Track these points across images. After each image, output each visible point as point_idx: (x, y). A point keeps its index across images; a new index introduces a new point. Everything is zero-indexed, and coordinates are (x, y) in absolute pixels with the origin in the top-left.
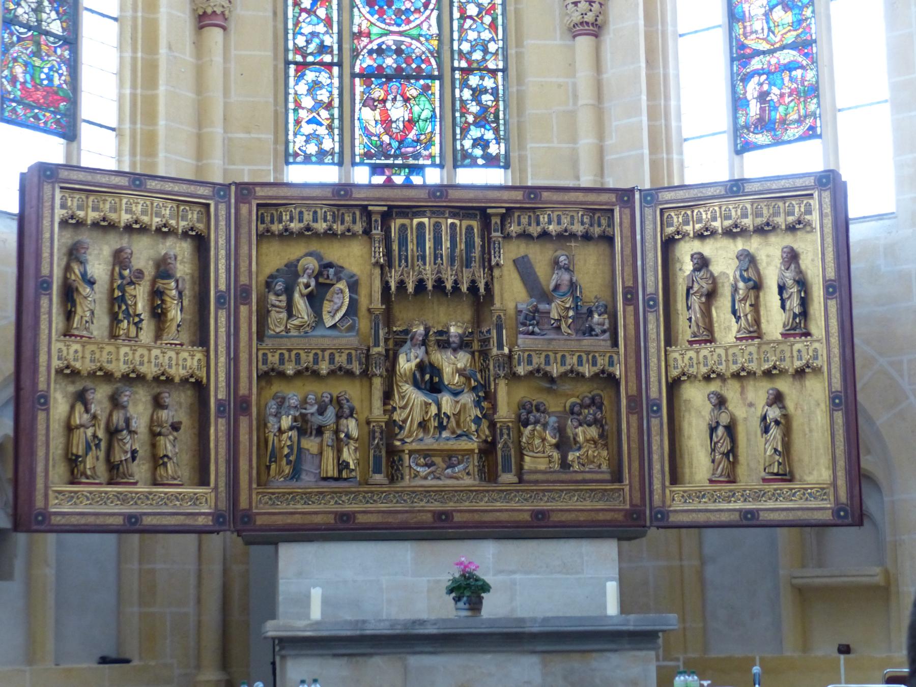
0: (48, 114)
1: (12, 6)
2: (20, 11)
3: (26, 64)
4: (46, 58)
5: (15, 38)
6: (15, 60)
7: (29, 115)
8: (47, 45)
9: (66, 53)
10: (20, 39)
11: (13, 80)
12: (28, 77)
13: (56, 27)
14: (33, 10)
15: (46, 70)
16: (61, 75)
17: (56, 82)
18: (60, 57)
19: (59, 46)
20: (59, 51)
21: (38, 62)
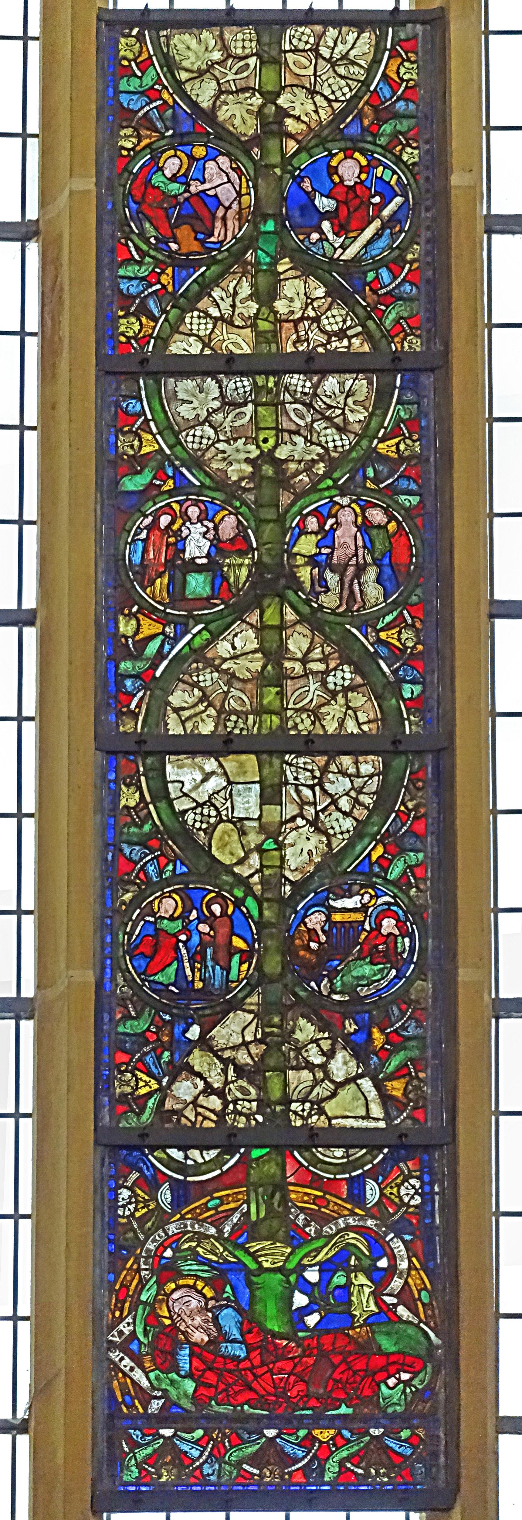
0: (324, 1435)
1: (147, 1085)
2: (185, 1089)
3: (220, 1275)
4: (311, 1230)
5: (165, 1195)
6: (167, 1272)
7: (234, 1455)
8: (316, 1182)
9: (409, 1193)
10: (183, 1194)
11: (165, 1344)
12: (229, 1319)
13: (357, 1107)
14: (240, 1071)
15: (312, 1276)
16: (380, 1280)
17: (364, 1303)
18: (379, 1210)
19: (373, 1174)
20: (372, 1192)
21: (272, 1254)
